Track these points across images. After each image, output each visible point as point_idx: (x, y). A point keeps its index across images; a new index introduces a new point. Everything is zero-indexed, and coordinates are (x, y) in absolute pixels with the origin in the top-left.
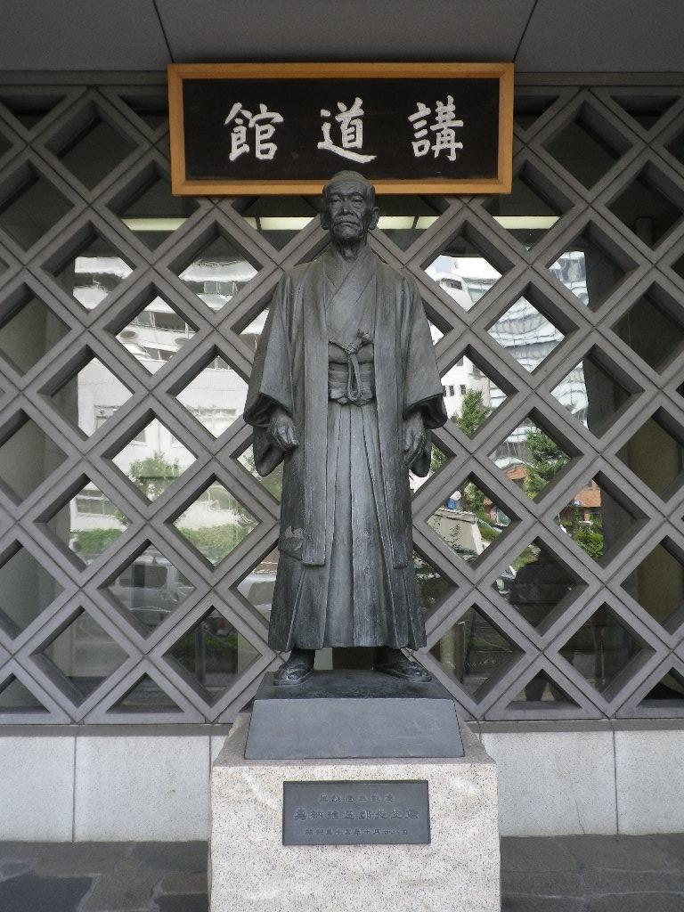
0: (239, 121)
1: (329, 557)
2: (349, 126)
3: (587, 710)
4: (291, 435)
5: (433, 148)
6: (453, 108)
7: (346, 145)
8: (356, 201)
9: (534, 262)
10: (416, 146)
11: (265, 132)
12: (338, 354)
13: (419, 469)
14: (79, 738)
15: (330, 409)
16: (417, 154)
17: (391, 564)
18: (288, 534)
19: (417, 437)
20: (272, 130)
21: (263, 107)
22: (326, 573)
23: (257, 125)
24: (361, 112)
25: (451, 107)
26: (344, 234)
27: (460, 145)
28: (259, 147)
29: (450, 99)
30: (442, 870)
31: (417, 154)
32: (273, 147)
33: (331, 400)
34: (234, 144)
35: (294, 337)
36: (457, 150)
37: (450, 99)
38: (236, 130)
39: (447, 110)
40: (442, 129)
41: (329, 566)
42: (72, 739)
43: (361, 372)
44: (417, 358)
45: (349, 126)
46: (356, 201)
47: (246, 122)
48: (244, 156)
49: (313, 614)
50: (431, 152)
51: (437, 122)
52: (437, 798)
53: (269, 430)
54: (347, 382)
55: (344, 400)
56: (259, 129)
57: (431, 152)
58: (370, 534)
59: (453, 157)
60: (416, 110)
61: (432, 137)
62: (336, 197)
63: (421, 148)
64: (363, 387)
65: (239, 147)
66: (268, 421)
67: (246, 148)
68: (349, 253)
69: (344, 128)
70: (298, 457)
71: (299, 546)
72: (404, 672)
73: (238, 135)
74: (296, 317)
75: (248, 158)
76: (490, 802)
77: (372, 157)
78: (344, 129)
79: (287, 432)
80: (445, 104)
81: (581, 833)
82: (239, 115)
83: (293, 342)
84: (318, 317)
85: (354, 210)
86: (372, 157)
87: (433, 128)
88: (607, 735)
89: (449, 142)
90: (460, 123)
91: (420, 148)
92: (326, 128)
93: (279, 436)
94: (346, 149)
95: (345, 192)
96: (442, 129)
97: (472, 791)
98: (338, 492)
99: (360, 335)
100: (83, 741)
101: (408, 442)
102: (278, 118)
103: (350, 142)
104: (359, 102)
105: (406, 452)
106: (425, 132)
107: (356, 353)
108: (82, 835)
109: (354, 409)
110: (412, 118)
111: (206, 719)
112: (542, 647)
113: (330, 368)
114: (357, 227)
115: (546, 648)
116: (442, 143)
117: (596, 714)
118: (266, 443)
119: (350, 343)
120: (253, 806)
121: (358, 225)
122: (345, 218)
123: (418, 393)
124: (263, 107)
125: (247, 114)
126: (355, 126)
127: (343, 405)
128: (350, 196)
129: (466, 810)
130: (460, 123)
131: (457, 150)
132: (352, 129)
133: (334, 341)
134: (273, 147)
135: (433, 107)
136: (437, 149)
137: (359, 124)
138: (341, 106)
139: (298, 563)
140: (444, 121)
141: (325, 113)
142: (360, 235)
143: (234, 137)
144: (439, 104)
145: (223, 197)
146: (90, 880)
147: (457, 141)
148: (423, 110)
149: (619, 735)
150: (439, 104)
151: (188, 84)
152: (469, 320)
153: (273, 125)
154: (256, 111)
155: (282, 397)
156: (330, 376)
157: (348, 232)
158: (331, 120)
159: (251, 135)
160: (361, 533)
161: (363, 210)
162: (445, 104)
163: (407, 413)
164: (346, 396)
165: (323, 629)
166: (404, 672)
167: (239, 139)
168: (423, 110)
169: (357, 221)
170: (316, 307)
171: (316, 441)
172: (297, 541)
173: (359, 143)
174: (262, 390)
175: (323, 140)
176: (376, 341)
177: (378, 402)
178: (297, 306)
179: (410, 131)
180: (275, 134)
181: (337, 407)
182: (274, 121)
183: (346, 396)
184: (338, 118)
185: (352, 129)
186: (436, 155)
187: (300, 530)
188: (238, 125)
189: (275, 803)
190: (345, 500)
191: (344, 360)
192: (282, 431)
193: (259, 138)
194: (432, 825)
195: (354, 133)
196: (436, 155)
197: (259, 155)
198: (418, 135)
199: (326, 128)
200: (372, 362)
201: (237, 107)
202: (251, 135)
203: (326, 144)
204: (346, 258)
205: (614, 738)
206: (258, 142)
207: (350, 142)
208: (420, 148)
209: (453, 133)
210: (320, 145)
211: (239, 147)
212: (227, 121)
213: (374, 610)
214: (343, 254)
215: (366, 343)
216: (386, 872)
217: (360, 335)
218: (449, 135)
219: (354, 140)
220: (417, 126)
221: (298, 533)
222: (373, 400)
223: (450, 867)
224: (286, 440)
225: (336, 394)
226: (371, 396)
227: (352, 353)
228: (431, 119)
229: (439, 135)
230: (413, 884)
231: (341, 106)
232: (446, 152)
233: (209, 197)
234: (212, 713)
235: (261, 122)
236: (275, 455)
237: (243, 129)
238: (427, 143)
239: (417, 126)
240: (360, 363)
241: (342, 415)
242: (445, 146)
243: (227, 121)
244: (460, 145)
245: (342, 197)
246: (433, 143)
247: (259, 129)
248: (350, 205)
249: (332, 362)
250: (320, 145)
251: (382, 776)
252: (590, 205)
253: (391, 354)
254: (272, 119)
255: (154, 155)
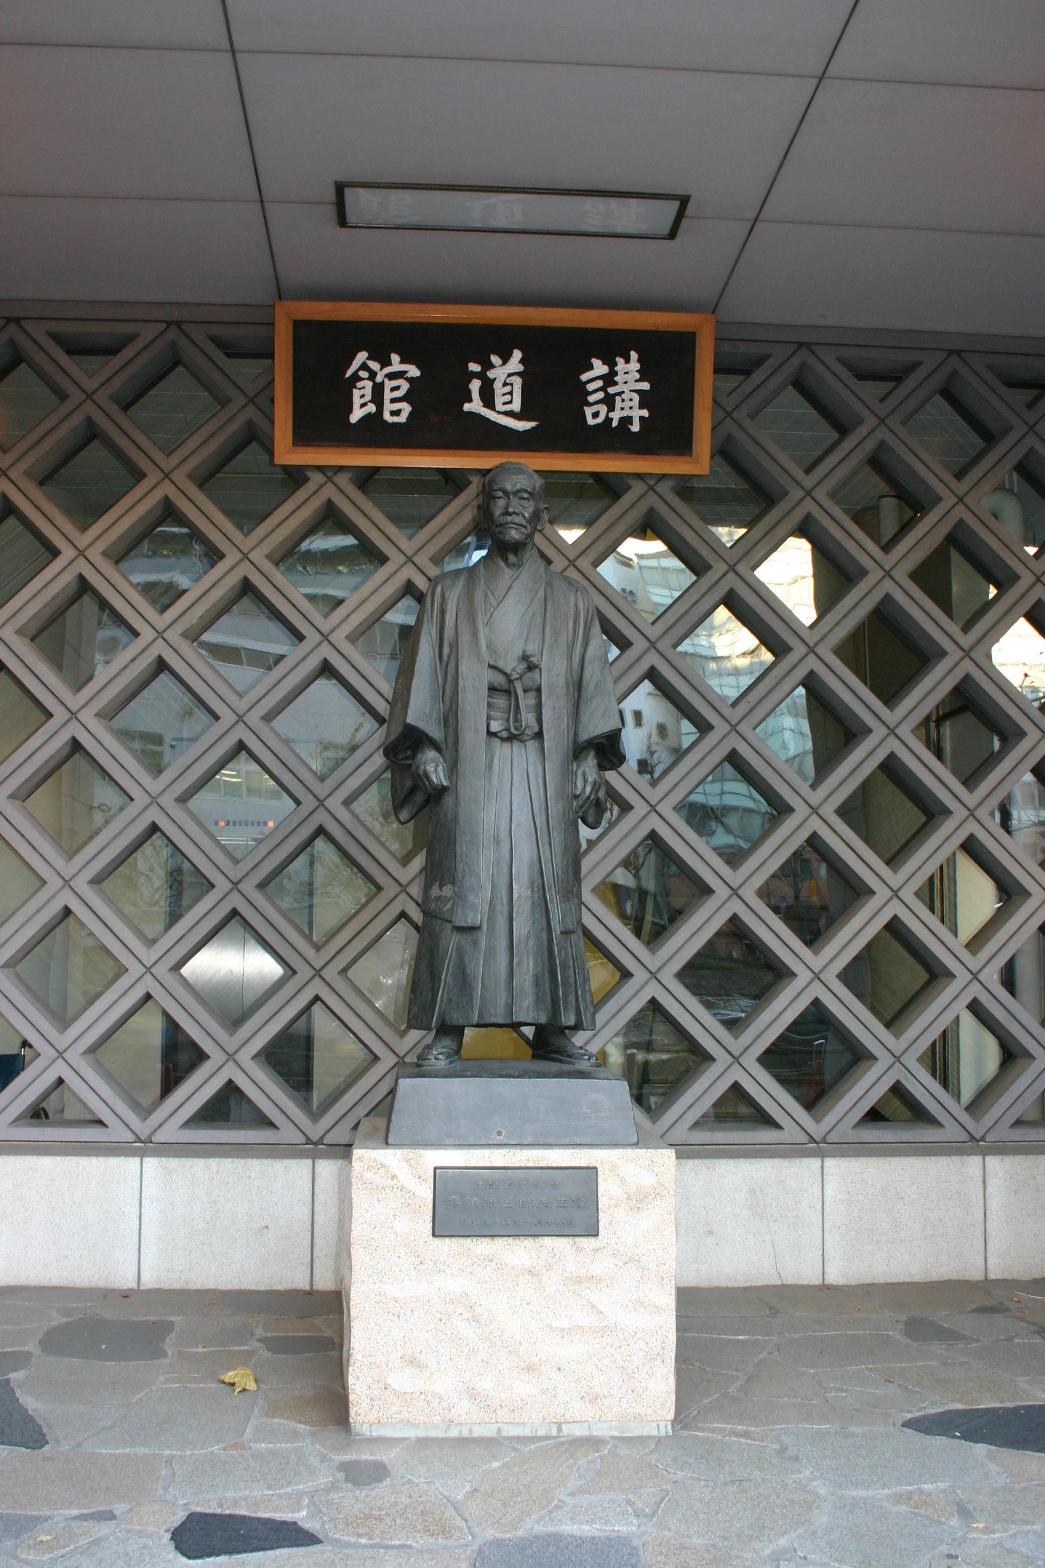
0: (364, 374)
1: (485, 919)
2: (505, 384)
3: (790, 1133)
4: (441, 774)
5: (611, 415)
6: (638, 366)
7: (499, 407)
8: (524, 499)
9: (735, 564)
10: (589, 411)
11: (396, 388)
12: (499, 679)
13: (590, 819)
14: (146, 1160)
15: (488, 744)
16: (591, 421)
17: (557, 928)
18: (435, 892)
19: (590, 779)
20: (405, 386)
21: (395, 358)
22: (483, 938)
23: (386, 381)
24: (520, 368)
25: (634, 366)
26: (507, 538)
27: (645, 413)
28: (388, 407)
29: (634, 355)
30: (612, 1266)
31: (591, 421)
32: (406, 408)
33: (490, 733)
34: (357, 401)
35: (445, 658)
36: (641, 418)
37: (634, 355)
38: (359, 385)
39: (628, 370)
40: (623, 392)
41: (485, 927)
42: (137, 1160)
43: (526, 702)
44: (592, 685)
45: (505, 384)
46: (524, 499)
47: (373, 375)
48: (368, 416)
49: (464, 982)
50: (608, 420)
51: (616, 383)
52: (607, 1189)
53: (413, 769)
54: (509, 713)
55: (505, 734)
56: (389, 384)
57: (608, 420)
58: (533, 892)
59: (635, 428)
60: (591, 367)
61: (609, 401)
62: (500, 494)
63: (596, 415)
64: (528, 718)
65: (363, 405)
66: (413, 757)
67: (372, 408)
68: (512, 558)
69: (498, 386)
70: (448, 800)
71: (449, 906)
72: (570, 1056)
73: (362, 392)
74: (449, 633)
75: (373, 421)
76: (666, 1192)
77: (533, 424)
78: (499, 389)
79: (436, 770)
80: (627, 361)
81: (779, 1282)
82: (364, 367)
83: (444, 663)
84: (475, 635)
85: (519, 509)
86: (533, 424)
87: (611, 390)
88: (815, 1163)
89: (631, 408)
90: (645, 386)
91: (593, 415)
92: (475, 385)
93: (426, 775)
94: (499, 413)
95: (509, 487)
96: (623, 392)
97: (647, 1180)
98: (497, 841)
99: (525, 657)
100: (150, 1162)
101: (580, 785)
102: (414, 371)
103: (504, 404)
104: (517, 355)
105: (576, 797)
106: (600, 395)
107: (520, 678)
108: (149, 1281)
109: (516, 744)
110: (585, 377)
111: (308, 1138)
112: (736, 1054)
113: (489, 696)
114: (523, 530)
115: (741, 1055)
116: (622, 409)
117: (804, 1138)
118: (409, 783)
119: (511, 664)
120: (399, 1193)
121: (525, 527)
122: (509, 518)
123: (595, 726)
124: (395, 358)
125: (374, 366)
126: (512, 385)
127: (503, 740)
128: (516, 493)
129: (638, 1201)
130: (645, 386)
131: (641, 418)
132: (508, 389)
133: (494, 664)
134: (406, 408)
135: (612, 365)
136: (616, 416)
137: (518, 382)
138: (495, 359)
139: (449, 926)
140: (626, 382)
141: (474, 367)
142: (526, 539)
143: (356, 393)
144: (620, 361)
145: (341, 469)
146: (172, 1323)
147: (641, 407)
148: (599, 368)
149: (830, 1162)
150: (620, 361)
151: (300, 326)
152: (653, 633)
153: (408, 380)
154: (386, 362)
155: (435, 731)
156: (489, 705)
157: (514, 535)
158: (482, 376)
159: (378, 391)
160: (521, 890)
161: (531, 510)
162: (627, 361)
163: (578, 751)
164: (508, 729)
165: (477, 1003)
166: (570, 1056)
167: (362, 396)
168: (599, 368)
169: (524, 523)
170: (473, 621)
171: (472, 785)
172: (446, 900)
173: (516, 406)
174: (409, 720)
175: (470, 400)
176: (544, 666)
177: (546, 737)
178: (449, 621)
179: (581, 393)
180: (409, 391)
181: (496, 742)
182: (409, 375)
183: (508, 729)
184: (491, 374)
185: (508, 389)
186: (615, 424)
187: (449, 886)
188: (362, 379)
189: (426, 1193)
190: (506, 852)
191: (505, 686)
192: (430, 768)
193: (388, 395)
194: (602, 1216)
195: (511, 393)
196: (615, 424)
197: (387, 417)
198: (591, 399)
199: (475, 385)
200: (539, 690)
201: (362, 356)
202: (378, 391)
203: (475, 406)
204: (508, 565)
205: (822, 1167)
206: (387, 402)
207: (504, 404)
208: (593, 415)
209: (636, 398)
210: (467, 407)
211: (363, 405)
212: (349, 373)
213: (537, 982)
214: (506, 560)
215: (531, 667)
216: (549, 1268)
217: (525, 657)
218: (631, 400)
219: (510, 402)
220: (591, 387)
221: (447, 891)
222: (539, 735)
223: (620, 1264)
224: (435, 780)
225: (495, 726)
226: (536, 730)
227: (517, 679)
228: (609, 379)
229: (618, 398)
230: (579, 1281)
231: (495, 359)
232: (626, 421)
233: (320, 469)
234: (315, 1131)
235: (392, 376)
236: (419, 798)
237: (369, 384)
238: (603, 409)
239: (591, 387)
240: (525, 691)
241: (502, 751)
242: (625, 413)
243: (349, 373)
244: (645, 413)
245: (506, 493)
246: (611, 408)
247: (389, 384)
248: (515, 505)
249: (493, 689)
250: (467, 407)
251: (545, 1162)
252: (808, 493)
253: (562, 681)
254: (406, 372)
255: (251, 412)
